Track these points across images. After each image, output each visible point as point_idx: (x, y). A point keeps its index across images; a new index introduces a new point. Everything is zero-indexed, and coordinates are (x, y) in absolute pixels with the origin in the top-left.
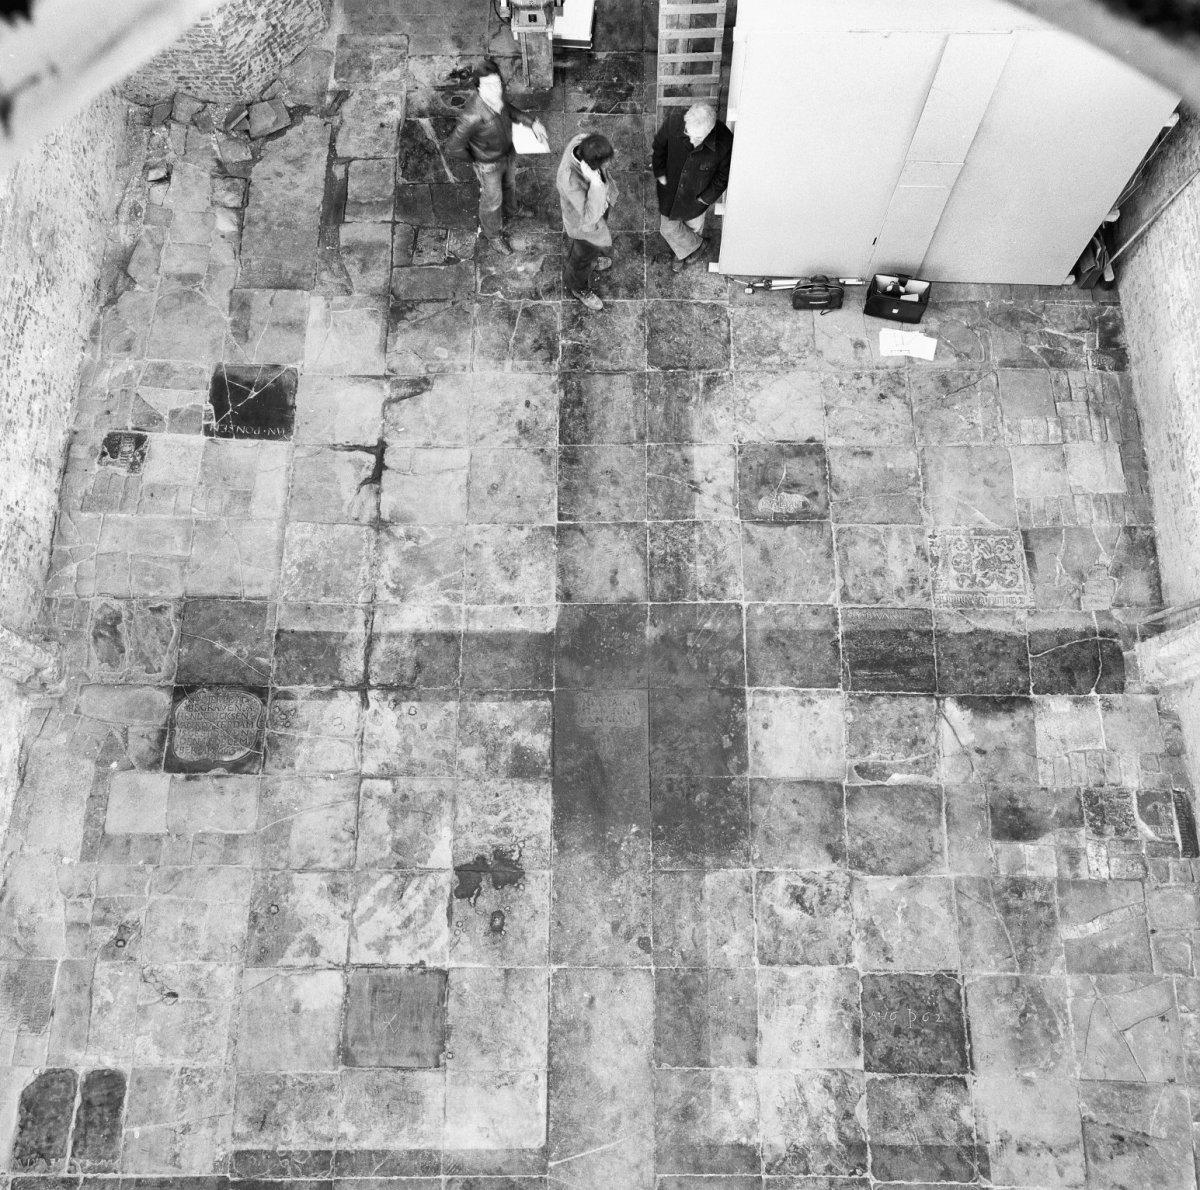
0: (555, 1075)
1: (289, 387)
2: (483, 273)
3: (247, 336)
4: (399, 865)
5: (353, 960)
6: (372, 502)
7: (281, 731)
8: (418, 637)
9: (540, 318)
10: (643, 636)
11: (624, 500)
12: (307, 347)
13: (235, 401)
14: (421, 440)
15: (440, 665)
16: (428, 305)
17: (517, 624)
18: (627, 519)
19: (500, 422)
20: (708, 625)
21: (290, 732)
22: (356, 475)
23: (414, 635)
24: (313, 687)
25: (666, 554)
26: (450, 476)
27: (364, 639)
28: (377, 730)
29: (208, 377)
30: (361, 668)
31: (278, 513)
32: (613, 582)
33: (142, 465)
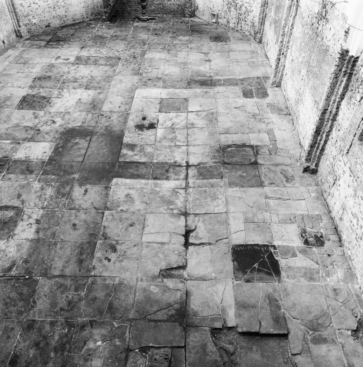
0: (132, 98)
1: (238, 270)
2: (125, 340)
3: (269, 299)
4: (173, 129)
5: (186, 113)
6: (189, 223)
7: (217, 154)
8: (167, 178)
9: (93, 308)
10: (80, 175)
11: (72, 218)
12: (232, 294)
13: (264, 261)
14: (166, 247)
15: (158, 172)
16: (162, 319)
17: (128, 181)
18: (74, 211)
19: (125, 252)
20: (53, 177)
21: (212, 154)
22: (198, 233)
23: (169, 179)
24: (206, 165)
25: (61, 198)
26: (152, 231)
27: (189, 179)
28: (182, 156)
29: (283, 274)
30: (189, 171)
31: (231, 215)
32: (86, 191)
33: (300, 232)
